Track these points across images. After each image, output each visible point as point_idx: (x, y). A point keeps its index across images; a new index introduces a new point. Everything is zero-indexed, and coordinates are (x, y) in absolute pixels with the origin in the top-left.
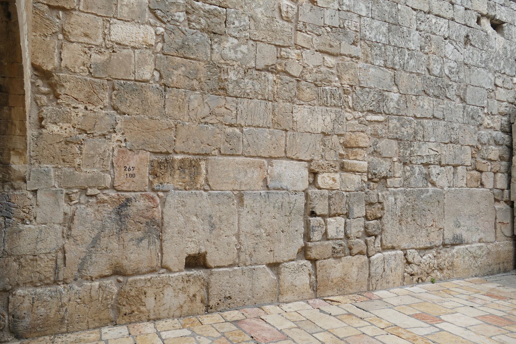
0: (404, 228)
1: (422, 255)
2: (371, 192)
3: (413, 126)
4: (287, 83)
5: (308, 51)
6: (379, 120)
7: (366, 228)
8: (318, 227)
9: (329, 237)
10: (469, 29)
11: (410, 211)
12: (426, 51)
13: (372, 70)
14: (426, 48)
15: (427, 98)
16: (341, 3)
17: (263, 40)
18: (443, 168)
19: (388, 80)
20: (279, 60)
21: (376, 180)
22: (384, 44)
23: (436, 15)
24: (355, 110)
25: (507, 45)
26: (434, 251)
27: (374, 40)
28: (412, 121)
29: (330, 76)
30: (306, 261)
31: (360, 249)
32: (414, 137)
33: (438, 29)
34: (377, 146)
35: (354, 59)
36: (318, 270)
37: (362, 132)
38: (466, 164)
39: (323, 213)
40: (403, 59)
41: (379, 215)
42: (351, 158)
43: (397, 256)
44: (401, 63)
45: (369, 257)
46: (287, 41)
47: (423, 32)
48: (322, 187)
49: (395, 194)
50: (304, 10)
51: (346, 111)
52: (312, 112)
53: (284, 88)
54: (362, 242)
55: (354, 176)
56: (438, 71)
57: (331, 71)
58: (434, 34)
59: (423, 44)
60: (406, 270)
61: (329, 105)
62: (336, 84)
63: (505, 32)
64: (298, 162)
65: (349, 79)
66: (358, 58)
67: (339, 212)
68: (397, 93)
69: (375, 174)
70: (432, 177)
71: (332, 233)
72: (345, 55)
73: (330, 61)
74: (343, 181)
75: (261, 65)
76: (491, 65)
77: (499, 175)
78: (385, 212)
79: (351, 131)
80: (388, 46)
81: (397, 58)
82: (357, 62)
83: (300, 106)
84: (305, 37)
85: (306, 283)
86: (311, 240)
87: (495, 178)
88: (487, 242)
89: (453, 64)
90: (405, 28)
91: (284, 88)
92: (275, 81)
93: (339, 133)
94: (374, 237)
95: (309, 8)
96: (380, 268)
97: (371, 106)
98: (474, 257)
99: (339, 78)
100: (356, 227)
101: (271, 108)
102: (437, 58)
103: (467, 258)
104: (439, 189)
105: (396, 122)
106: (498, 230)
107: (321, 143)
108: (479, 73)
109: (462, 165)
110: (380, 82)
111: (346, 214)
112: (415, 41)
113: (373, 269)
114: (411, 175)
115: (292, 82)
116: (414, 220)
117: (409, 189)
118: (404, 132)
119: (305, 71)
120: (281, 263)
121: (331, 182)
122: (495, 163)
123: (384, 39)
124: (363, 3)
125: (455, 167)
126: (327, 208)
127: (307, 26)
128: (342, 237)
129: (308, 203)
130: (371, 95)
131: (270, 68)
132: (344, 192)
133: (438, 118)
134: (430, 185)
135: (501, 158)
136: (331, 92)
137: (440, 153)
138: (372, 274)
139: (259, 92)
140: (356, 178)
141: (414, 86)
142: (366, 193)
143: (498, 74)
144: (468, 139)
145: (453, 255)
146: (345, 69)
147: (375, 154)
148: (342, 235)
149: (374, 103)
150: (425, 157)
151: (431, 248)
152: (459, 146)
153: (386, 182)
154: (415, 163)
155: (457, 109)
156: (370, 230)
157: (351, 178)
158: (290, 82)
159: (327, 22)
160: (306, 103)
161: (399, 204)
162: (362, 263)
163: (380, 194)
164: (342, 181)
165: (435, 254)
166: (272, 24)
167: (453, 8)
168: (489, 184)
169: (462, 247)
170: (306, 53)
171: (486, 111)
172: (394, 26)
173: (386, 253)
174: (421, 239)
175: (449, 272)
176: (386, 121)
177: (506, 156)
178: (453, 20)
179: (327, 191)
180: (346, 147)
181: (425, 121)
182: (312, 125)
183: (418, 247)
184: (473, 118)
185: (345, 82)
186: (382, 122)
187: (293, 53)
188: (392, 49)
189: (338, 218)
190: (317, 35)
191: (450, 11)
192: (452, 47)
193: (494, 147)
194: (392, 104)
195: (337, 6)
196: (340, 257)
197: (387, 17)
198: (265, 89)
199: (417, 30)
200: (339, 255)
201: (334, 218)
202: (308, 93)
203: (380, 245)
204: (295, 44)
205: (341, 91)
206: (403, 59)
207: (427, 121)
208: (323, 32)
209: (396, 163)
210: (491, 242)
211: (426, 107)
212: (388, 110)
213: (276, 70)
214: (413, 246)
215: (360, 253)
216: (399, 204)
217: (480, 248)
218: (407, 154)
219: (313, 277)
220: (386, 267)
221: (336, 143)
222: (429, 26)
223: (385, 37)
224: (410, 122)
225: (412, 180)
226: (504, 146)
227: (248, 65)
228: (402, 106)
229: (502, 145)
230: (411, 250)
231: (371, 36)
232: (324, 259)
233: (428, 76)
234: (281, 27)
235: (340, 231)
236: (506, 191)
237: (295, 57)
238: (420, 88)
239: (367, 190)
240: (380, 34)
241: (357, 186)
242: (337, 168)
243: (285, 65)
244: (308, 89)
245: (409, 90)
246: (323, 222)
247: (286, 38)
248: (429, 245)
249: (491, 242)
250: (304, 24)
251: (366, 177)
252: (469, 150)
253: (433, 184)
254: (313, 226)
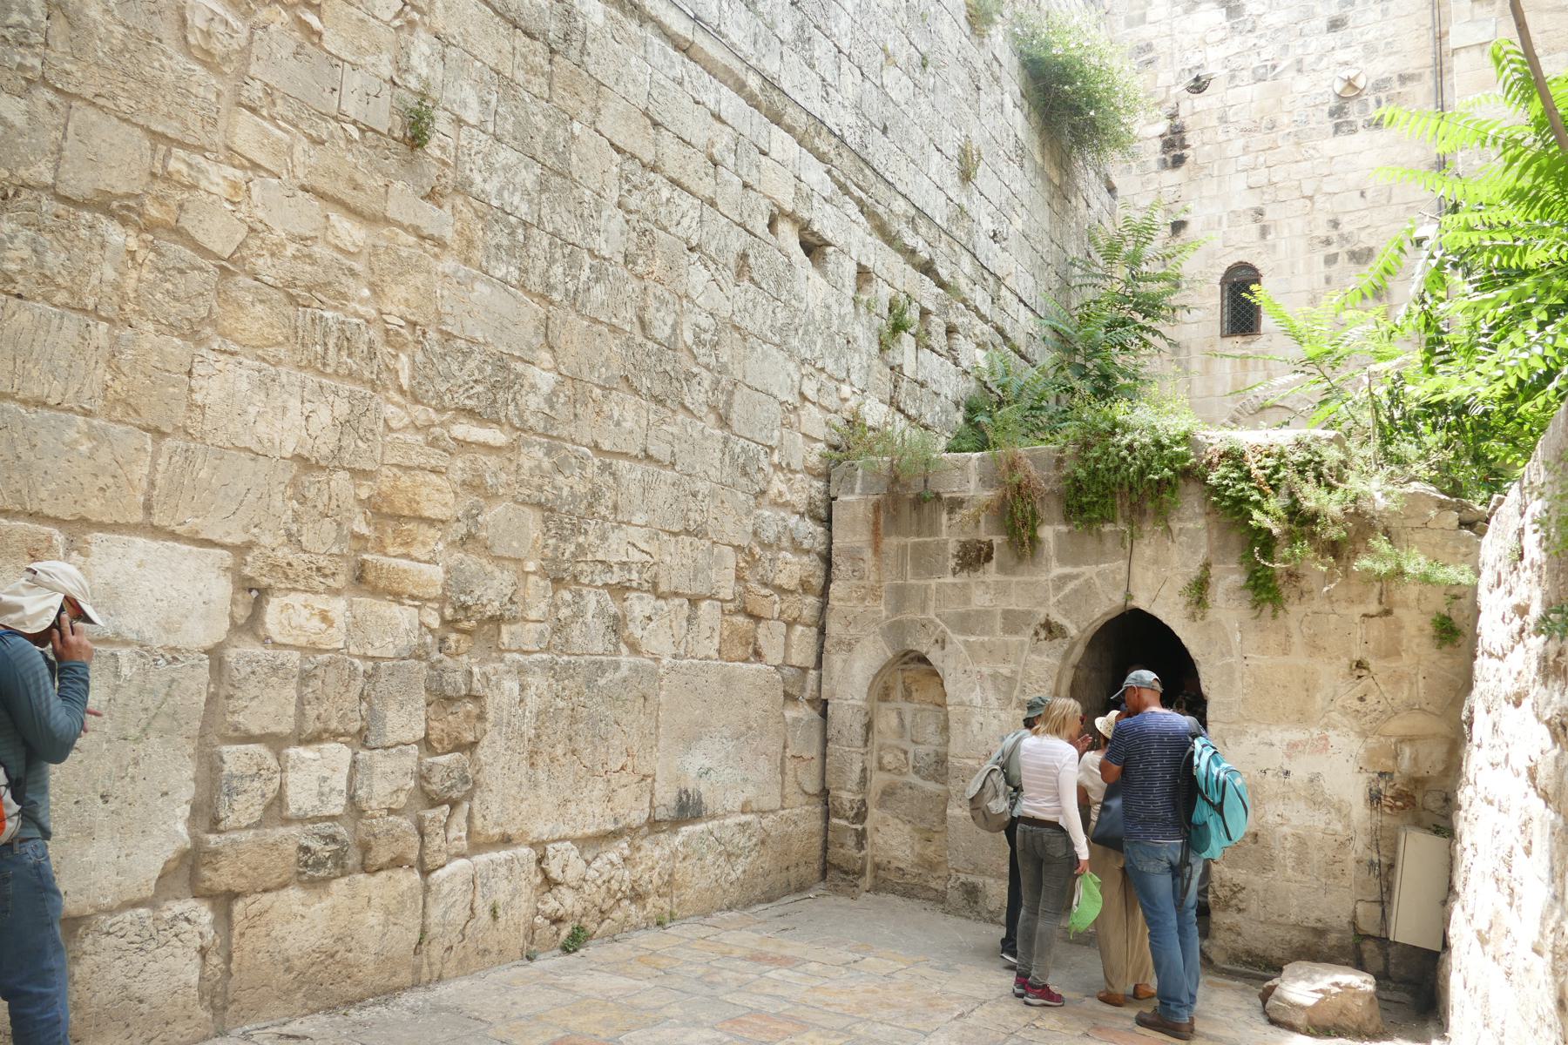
0: (542, 776)
1: (589, 857)
2: (449, 662)
3: (589, 472)
4: (181, 272)
5: (275, 181)
6: (492, 442)
7: (423, 777)
8: (252, 778)
9: (292, 810)
10: (750, 239)
11: (563, 723)
12: (639, 269)
13: (481, 289)
14: (640, 261)
15: (632, 400)
16: (402, 65)
17: (100, 101)
18: (662, 602)
19: (528, 330)
20: (159, 186)
21: (465, 625)
22: (524, 223)
23: (672, 181)
24: (417, 401)
25: (831, 301)
26: (623, 845)
27: (495, 203)
29: (343, 279)
30: (192, 903)
31: (398, 848)
32: (590, 505)
33: (676, 217)
34: (480, 519)
35: (428, 245)
36: (236, 932)
37: (433, 471)
38: (721, 596)
39: (274, 729)
40: (574, 277)
41: (469, 737)
42: (390, 550)
43: (516, 866)
44: (569, 286)
45: (425, 873)
46: (198, 128)
47: (636, 217)
48: (278, 639)
49: (522, 670)
50: (274, 46)
51: (388, 400)
52: (265, 384)
53: (169, 286)
54: (406, 823)
55: (396, 607)
56: (668, 331)
57: (348, 263)
58: (665, 229)
59: (633, 249)
60: (539, 905)
61: (329, 370)
62: (362, 310)
63: (830, 267)
64: (195, 549)
65: (407, 300)
66: (441, 243)
67: (333, 725)
68: (549, 370)
69: (466, 608)
70: (631, 625)
71: (301, 798)
72: (401, 226)
73: (349, 231)
74: (356, 624)
75: (79, 182)
76: (795, 342)
77: (799, 628)
78: (488, 726)
79: (398, 466)
80: (535, 230)
81: (558, 270)
82: (436, 256)
83: (222, 357)
84: (267, 135)
85: (187, 985)
86: (221, 827)
87: (787, 637)
88: (762, 812)
89: (705, 322)
90: (588, 192)
91: (169, 286)
92: (132, 254)
93: (357, 466)
94: (446, 807)
95: (292, 46)
96: (459, 907)
97: (469, 397)
98: (729, 855)
99: (374, 292)
100: (389, 779)
101: (104, 342)
102: (667, 295)
103: (710, 858)
104: (648, 662)
105: (541, 454)
106: (790, 778)
107: (289, 492)
108: (766, 355)
109: (710, 598)
110: (503, 328)
111: (360, 731)
112: (611, 235)
113: (435, 913)
114: (575, 616)
115: (201, 269)
116: (574, 752)
117: (566, 658)
119: (254, 243)
120: (88, 917)
121: (316, 623)
122: (791, 598)
123: (524, 208)
124: (473, 87)
125: (694, 602)
126: (292, 710)
127: (279, 102)
128: (338, 811)
129: (222, 693)
130: (471, 364)
131: (115, 204)
132: (357, 661)
133: (658, 461)
134: (624, 649)
135: (805, 586)
136: (343, 331)
137: (656, 558)
138: (434, 930)
139: (60, 280)
140: (403, 616)
141: (600, 360)
142: (432, 667)
143: (807, 369)
144: (728, 527)
145: (674, 854)
146: (397, 270)
147: (469, 546)
148: (337, 805)
149: (479, 388)
150: (616, 568)
151: (615, 835)
152: (708, 543)
153: (499, 632)
154: (586, 581)
155: (708, 444)
156: (435, 786)
157: (388, 614)
158: (194, 268)
159: (351, 107)
160: (247, 350)
161: (533, 703)
162: (402, 895)
163: (476, 670)
164: (356, 625)
165: (626, 853)
166: (142, 58)
167: (716, 173)
168: (774, 655)
169: (700, 827)
170: (265, 187)
171: (776, 458)
172: (559, 179)
173: (482, 859)
174: (589, 811)
175: (661, 902)
176: (512, 447)
177: (817, 582)
178: (713, 204)
179: (296, 655)
180: (377, 512)
181: (622, 465)
182: (261, 428)
183: (579, 833)
184: (746, 474)
185: (394, 310)
186: (499, 448)
187: (218, 177)
188: (545, 242)
189: (330, 748)
190: (309, 137)
191: (707, 180)
192: (707, 275)
193: (789, 556)
194: (534, 402)
195: (387, 70)
196: (326, 880)
197: (539, 148)
198: (87, 274)
199: (620, 205)
200: (322, 873)
201: (315, 747)
202: (256, 319)
203: (464, 834)
204: (229, 148)
205: (375, 334)
206: (574, 277)
207: (627, 464)
208: (331, 135)
209: (532, 578)
210: (772, 811)
211: (627, 425)
212: (520, 416)
213: (139, 215)
214: (565, 830)
215: (397, 863)
216: (533, 703)
217: (743, 826)
218: (567, 555)
219: (215, 960)
220: (479, 902)
221: (342, 498)
222: (653, 204)
223: (530, 202)
224: (582, 461)
225: (576, 631)
226: (813, 556)
227: (23, 173)
228: (563, 411)
229: (808, 552)
230: (558, 845)
231: (487, 187)
232: (265, 891)
233: (639, 339)
234: (179, 78)
235: (332, 790)
236: (813, 674)
237: (222, 189)
238: (616, 370)
239: (436, 656)
240: (515, 189)
241: (402, 642)
242: (340, 581)
243: (181, 206)
244: (259, 307)
245: (585, 370)
246: (272, 762)
247: (194, 121)
248: (611, 827)
249: (772, 811)
250: (269, 91)
251: (436, 614)
252: (730, 559)
253: (634, 648)
254: (232, 776)
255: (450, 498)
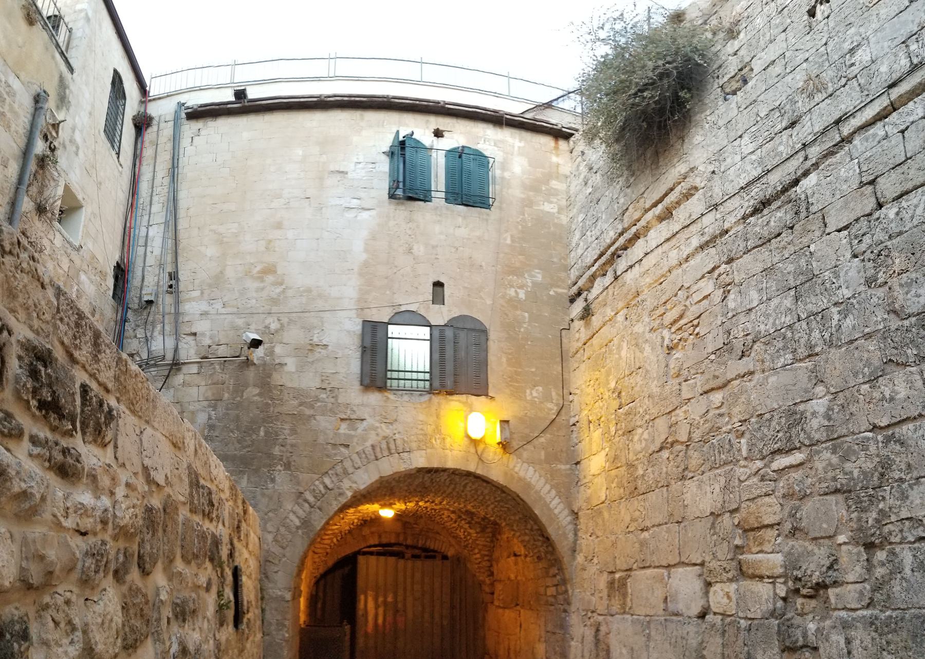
28: (868, 439)
34: (798, 515)
118: (851, 472)
147: (798, 535)
207: (911, 426)
218: (870, 522)
255: (777, 508)
